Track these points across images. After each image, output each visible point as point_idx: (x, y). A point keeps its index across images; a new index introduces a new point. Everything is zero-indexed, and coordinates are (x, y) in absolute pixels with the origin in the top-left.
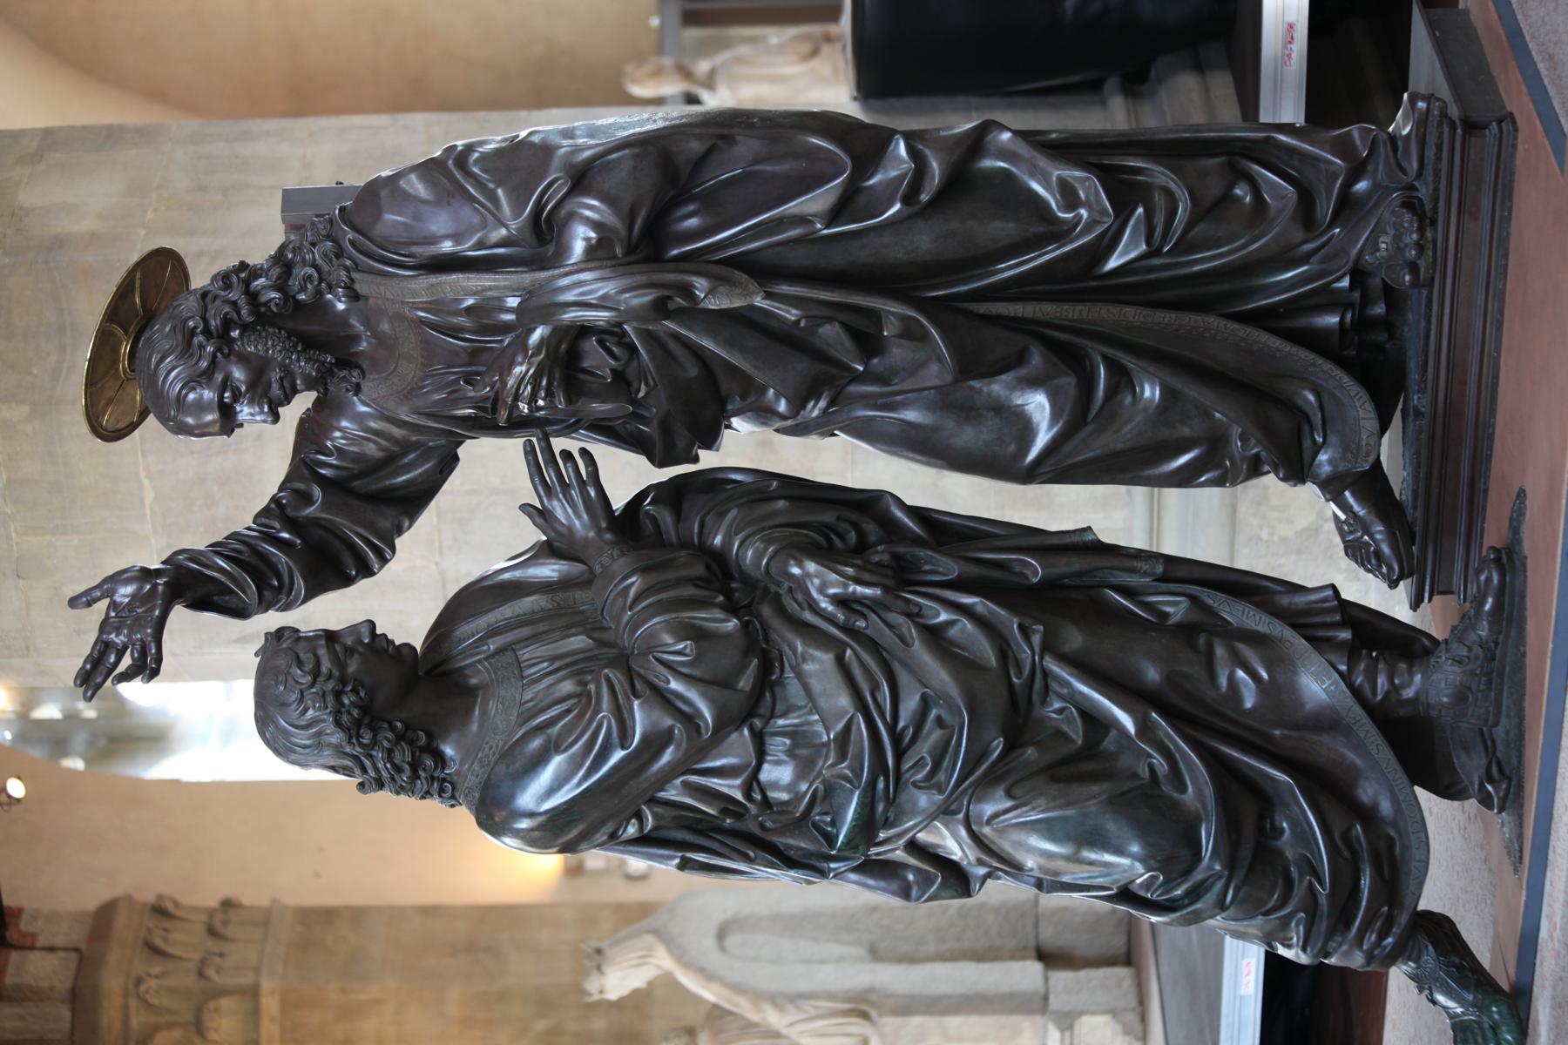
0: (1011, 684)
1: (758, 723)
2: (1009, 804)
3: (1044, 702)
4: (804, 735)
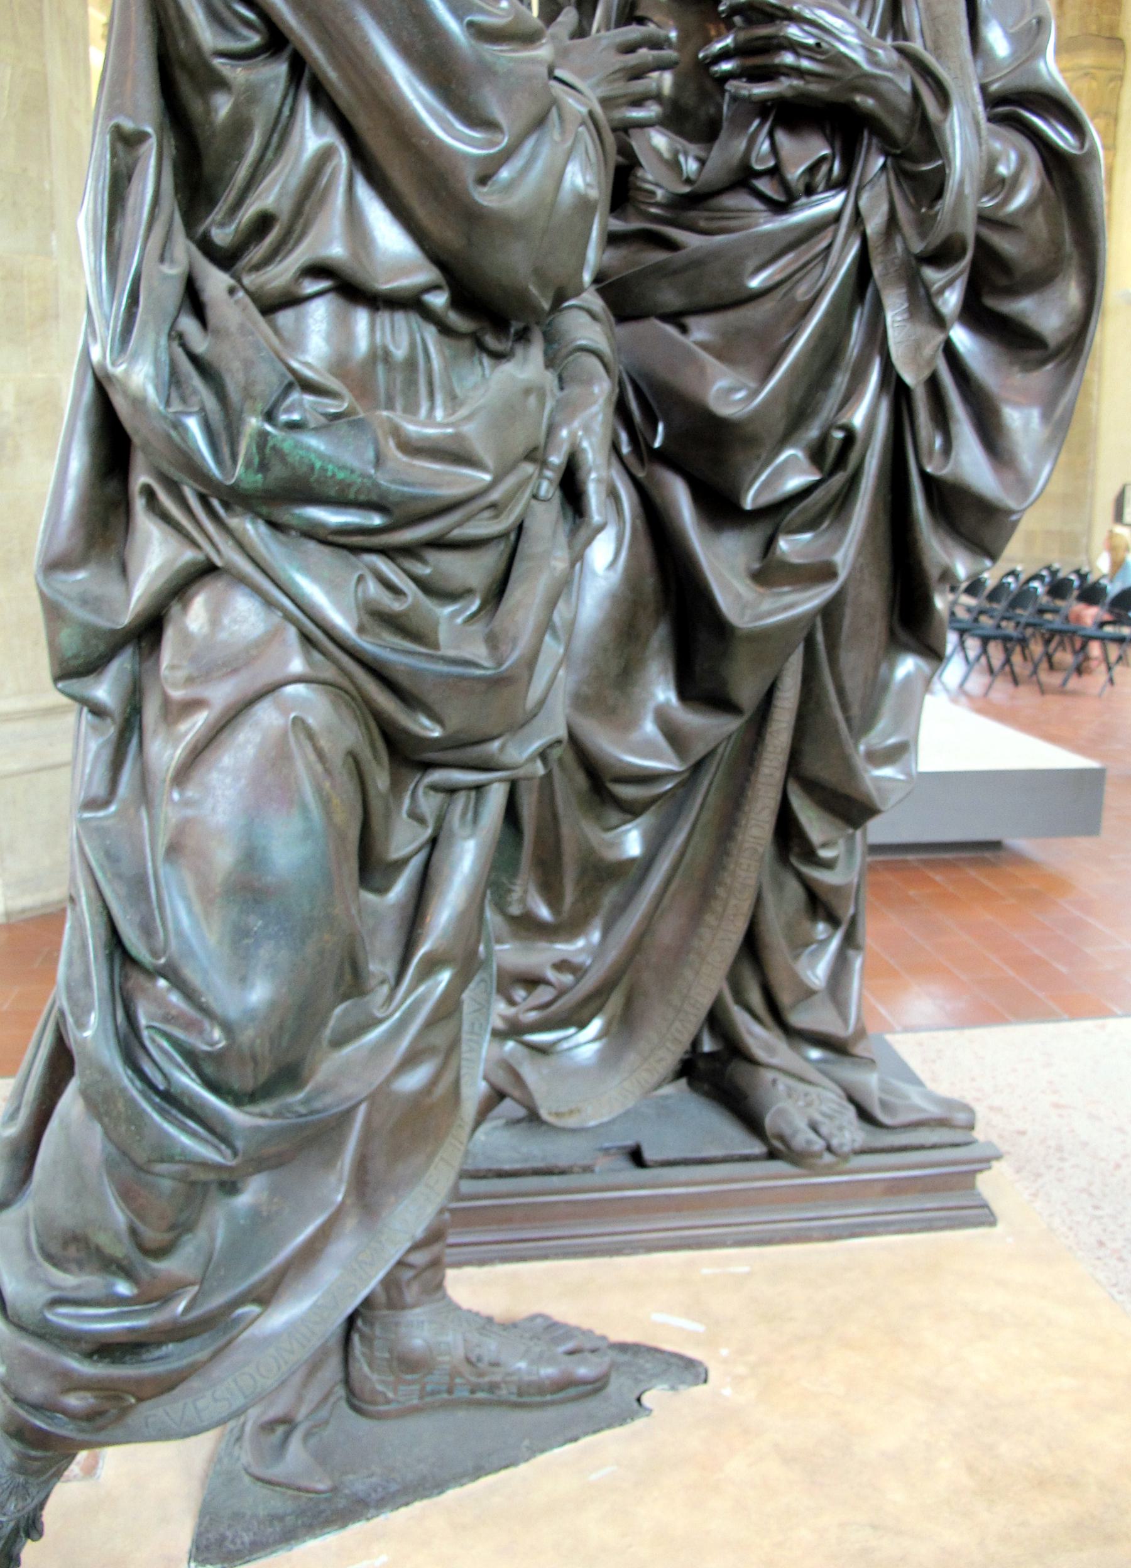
0: (492, 739)
1: (438, 300)
2: (337, 759)
3: (434, 788)
4: (411, 383)
